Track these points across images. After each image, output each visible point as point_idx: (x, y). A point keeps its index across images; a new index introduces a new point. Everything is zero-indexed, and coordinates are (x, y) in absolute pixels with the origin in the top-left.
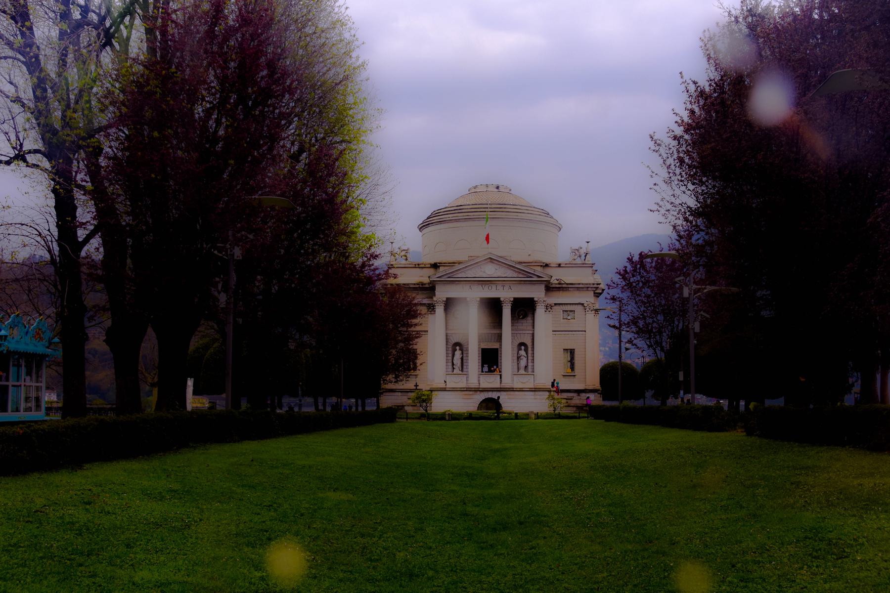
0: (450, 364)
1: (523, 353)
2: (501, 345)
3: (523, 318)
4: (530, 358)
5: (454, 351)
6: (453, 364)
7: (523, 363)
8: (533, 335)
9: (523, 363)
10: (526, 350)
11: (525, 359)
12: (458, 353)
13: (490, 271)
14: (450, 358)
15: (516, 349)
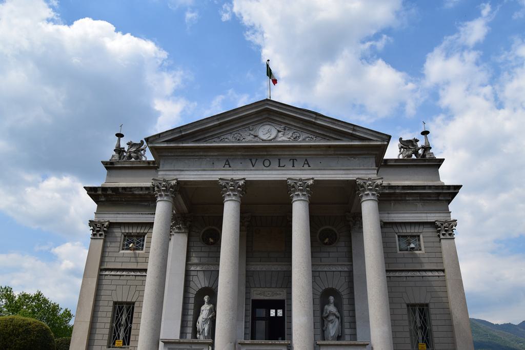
0: (189, 330)
1: (331, 308)
2: (289, 294)
3: (330, 244)
4: (346, 319)
5: (199, 304)
6: (195, 331)
7: (333, 329)
8: (350, 274)
9: (333, 329)
10: (338, 305)
11: (337, 322)
12: (205, 309)
13: (267, 134)
14: (190, 318)
15: (318, 301)
